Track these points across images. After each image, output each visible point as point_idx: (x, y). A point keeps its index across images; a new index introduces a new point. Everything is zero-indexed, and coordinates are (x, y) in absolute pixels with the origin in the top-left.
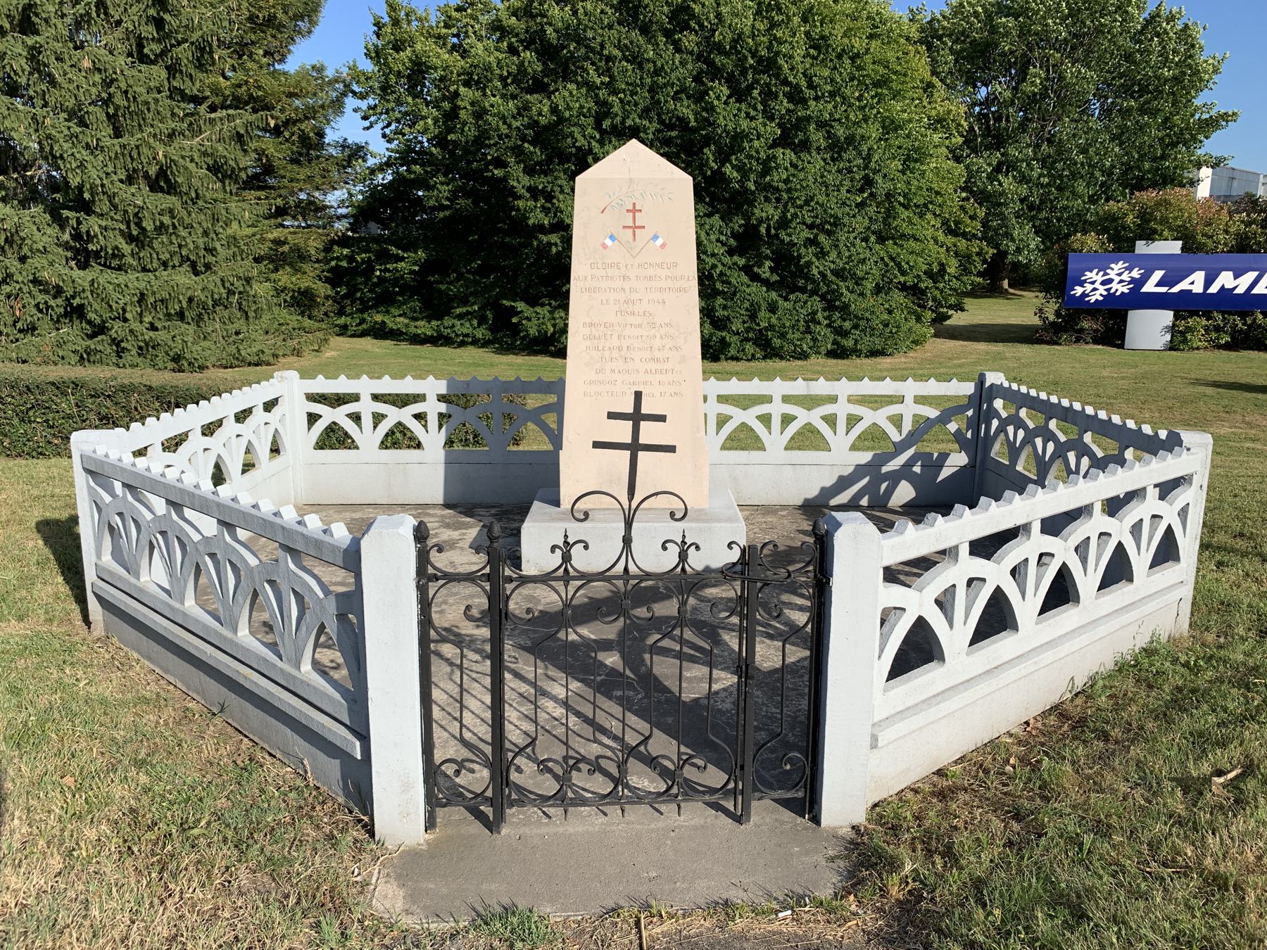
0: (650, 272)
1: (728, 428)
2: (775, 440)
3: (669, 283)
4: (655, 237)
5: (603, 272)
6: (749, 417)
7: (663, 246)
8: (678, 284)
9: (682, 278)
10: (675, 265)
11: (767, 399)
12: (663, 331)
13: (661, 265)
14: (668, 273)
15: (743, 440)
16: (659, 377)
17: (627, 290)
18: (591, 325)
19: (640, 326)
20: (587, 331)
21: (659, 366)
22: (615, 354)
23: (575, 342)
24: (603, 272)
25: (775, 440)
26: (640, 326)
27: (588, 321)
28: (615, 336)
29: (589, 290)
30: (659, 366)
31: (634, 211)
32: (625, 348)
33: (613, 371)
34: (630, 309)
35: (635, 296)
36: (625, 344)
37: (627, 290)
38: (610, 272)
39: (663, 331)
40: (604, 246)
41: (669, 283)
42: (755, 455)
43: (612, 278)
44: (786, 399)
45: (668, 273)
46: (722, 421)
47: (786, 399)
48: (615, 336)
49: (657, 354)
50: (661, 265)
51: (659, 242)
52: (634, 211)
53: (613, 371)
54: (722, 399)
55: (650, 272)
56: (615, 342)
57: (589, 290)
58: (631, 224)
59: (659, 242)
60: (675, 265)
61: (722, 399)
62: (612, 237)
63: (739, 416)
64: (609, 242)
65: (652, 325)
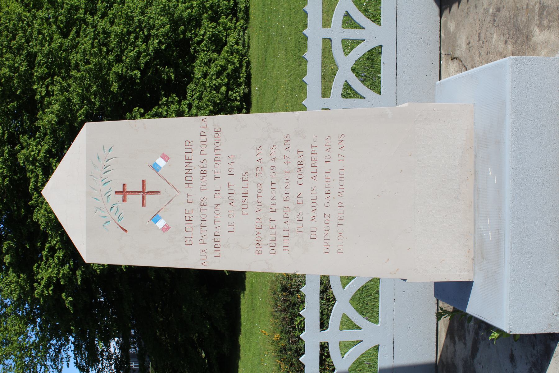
0: (196, 173)
1: (357, 85)
2: (371, 35)
3: (209, 150)
4: (155, 168)
5: (197, 233)
6: (345, 63)
7: (166, 158)
8: (211, 140)
9: (203, 135)
10: (188, 143)
11: (327, 42)
12: (266, 158)
13: (188, 161)
14: (196, 152)
15: (369, 69)
16: (320, 163)
17: (218, 201)
18: (258, 245)
19: (260, 185)
20: (266, 250)
21: (308, 163)
22: (292, 216)
23: (282, 264)
24: (197, 233)
25: (371, 35)
26: (260, 185)
27: (253, 249)
28: (273, 216)
29: (217, 248)
30: (308, 163)
31: (124, 192)
32: (286, 204)
33: (313, 218)
34: (238, 198)
35: (224, 193)
36: (280, 204)
37: (218, 201)
38: (196, 222)
39: (266, 158)
40: (166, 228)
41: (209, 150)
42: (386, 58)
43: (203, 219)
44: (327, 23)
45: (196, 152)
46: (349, 92)
47: (327, 23)
48: (273, 216)
49: (294, 164)
50: (188, 161)
51: (161, 162)
52: (124, 192)
53: (313, 218)
54: (326, 93)
55: (196, 173)
56: (279, 216)
57: (217, 248)
58: (140, 196)
59: (161, 162)
60: (188, 143)
61: (326, 93)
62: (155, 219)
63: (344, 74)
64: (161, 224)
65: (259, 171)
